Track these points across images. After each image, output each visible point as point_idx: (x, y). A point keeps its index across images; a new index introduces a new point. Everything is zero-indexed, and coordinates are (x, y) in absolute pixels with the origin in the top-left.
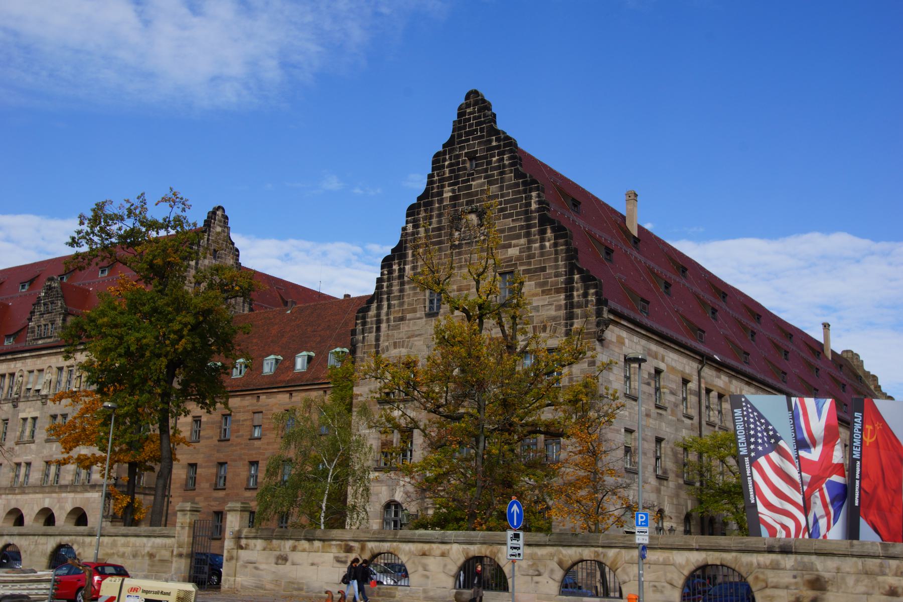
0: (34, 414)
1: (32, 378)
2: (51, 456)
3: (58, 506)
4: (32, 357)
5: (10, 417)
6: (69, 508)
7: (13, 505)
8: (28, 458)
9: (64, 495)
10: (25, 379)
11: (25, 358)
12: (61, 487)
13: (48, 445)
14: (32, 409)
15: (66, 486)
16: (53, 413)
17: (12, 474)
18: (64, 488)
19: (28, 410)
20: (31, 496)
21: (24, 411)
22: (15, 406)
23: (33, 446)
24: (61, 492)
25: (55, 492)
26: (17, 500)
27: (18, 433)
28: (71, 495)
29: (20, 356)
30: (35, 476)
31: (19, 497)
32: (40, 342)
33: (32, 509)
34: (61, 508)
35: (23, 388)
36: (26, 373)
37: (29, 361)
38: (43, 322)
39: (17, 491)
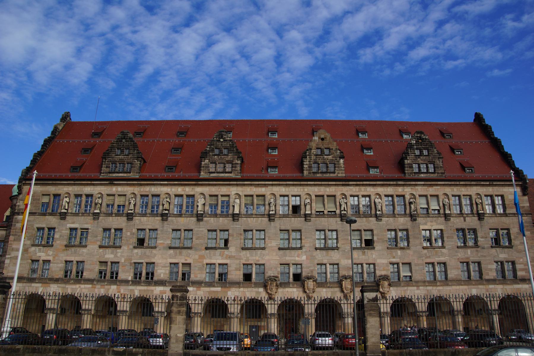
4: (424, 185)
5: (409, 227)
8: (442, 259)
9: (491, 286)
11: (416, 185)
13: (460, 250)
19: (429, 224)
20: (454, 287)
21: (425, 224)
23: (443, 250)
24: (488, 284)
25: (483, 284)
26: (439, 291)
28: (501, 286)
29: (410, 183)
31: (441, 288)
32: (422, 175)
37: (419, 188)
39: (438, 284)
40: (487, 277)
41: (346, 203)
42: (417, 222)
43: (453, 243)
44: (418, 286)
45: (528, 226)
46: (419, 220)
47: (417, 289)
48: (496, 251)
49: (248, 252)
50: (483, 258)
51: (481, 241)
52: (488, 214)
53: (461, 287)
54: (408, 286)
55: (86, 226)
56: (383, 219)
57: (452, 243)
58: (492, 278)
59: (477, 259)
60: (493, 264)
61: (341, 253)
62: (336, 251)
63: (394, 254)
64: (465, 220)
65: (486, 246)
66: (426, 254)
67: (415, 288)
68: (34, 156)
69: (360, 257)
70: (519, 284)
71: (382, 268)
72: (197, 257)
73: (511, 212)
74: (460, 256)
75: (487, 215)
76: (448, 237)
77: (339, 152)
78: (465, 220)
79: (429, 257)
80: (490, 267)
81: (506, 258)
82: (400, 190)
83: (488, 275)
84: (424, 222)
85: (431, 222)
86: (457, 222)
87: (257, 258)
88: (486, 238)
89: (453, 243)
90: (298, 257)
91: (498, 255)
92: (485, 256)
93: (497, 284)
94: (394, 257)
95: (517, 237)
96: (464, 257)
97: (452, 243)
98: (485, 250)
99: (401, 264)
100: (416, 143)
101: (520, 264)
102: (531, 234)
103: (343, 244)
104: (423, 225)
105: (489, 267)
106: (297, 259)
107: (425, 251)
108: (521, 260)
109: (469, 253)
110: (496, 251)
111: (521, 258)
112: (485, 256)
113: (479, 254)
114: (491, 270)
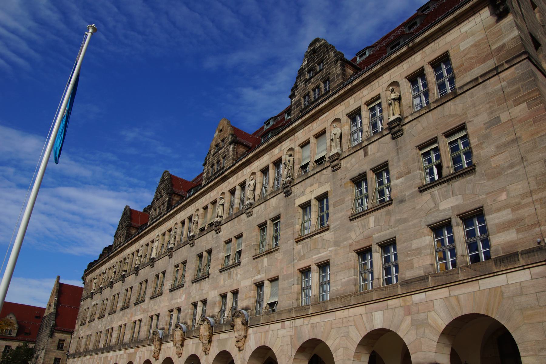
0: (320, 191)
1: (307, 151)
2: (370, 237)
3: (408, 320)
5: (282, 211)
6: (441, 319)
7: (307, 335)
8: (322, 256)
9: (417, 298)
10: (297, 156)
12: (407, 283)
13: (355, 223)
14: (316, 185)
15: (423, 279)
16: (355, 173)
17: (297, 288)
18: (420, 283)
19: (308, 190)
21: (303, 193)
22: (288, 194)
24: (410, 293)
25: (397, 296)
26: (313, 326)
27: (298, 227)
28: (443, 292)
30: (342, 279)
31: (315, 319)
33: (347, 336)
34: (417, 324)
35: (297, 167)
36: (298, 149)
38: (310, 86)
40: (408, 274)
41: (223, 205)
42: (292, 195)
43: (344, 213)
44: (283, 321)
45: (518, 91)
46: (296, 190)
47: (282, 328)
48: (433, 197)
49: (153, 301)
50: (400, 227)
51: (396, 185)
52: (411, 115)
53: (353, 311)
54: (269, 323)
55: (98, 301)
56: (255, 210)
57: (340, 215)
58: (421, 273)
59: (384, 235)
60: (423, 235)
61: (210, 281)
62: (207, 279)
63: (260, 265)
64: (366, 154)
65: (407, 193)
66: (299, 252)
67: (279, 325)
68: (104, 250)
69: (226, 283)
70: (495, 274)
71: (244, 296)
72: (129, 315)
73: (468, 79)
74: (354, 237)
75: (410, 118)
76: (335, 205)
77: (230, 137)
78: (366, 154)
79: (302, 258)
80: (415, 244)
81: (457, 206)
82: (276, 152)
83: (412, 267)
84: (302, 190)
85: (312, 185)
86: (353, 165)
87: (156, 307)
88: (409, 172)
89: (344, 213)
90: (180, 298)
91: (437, 205)
92: (405, 221)
93: (433, 288)
94: (259, 273)
95: (486, 137)
96: (361, 237)
97: (340, 215)
98: (406, 205)
99: (267, 283)
100: (308, 63)
101: (499, 210)
102: (529, 106)
103: (214, 268)
104: (300, 196)
105: (414, 246)
106: (179, 300)
107: (300, 246)
108: (504, 196)
109: (372, 225)
110: (433, 197)
111: (503, 189)
112: (405, 221)
113: (393, 219)
114: (418, 251)
